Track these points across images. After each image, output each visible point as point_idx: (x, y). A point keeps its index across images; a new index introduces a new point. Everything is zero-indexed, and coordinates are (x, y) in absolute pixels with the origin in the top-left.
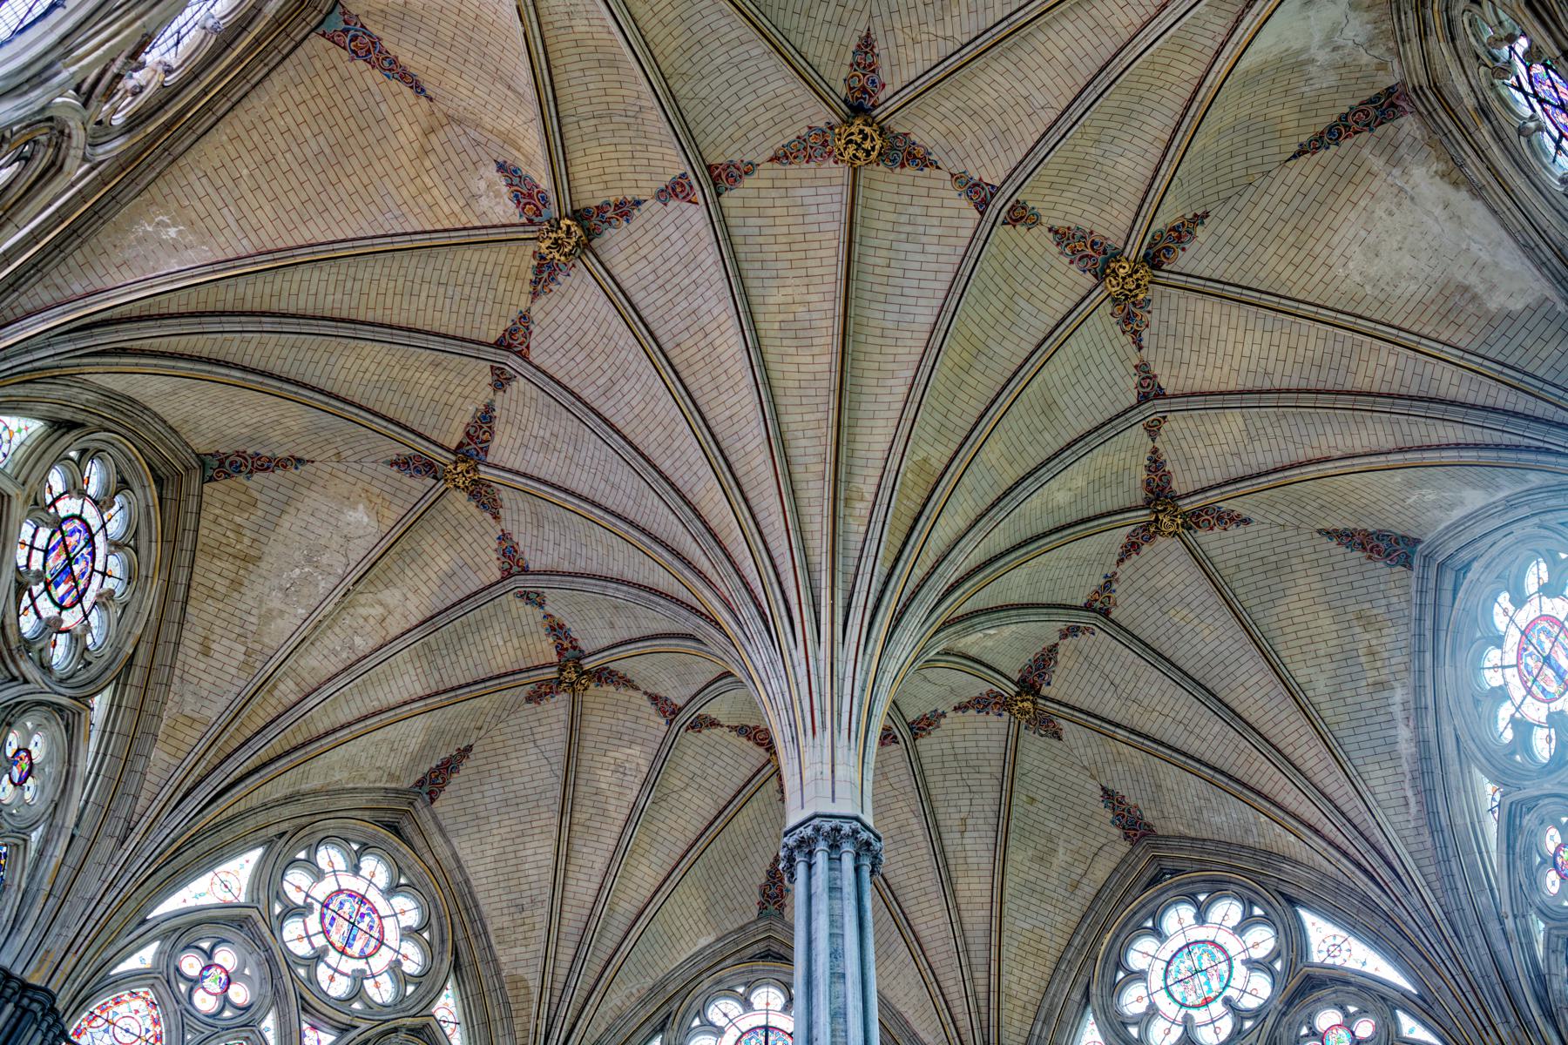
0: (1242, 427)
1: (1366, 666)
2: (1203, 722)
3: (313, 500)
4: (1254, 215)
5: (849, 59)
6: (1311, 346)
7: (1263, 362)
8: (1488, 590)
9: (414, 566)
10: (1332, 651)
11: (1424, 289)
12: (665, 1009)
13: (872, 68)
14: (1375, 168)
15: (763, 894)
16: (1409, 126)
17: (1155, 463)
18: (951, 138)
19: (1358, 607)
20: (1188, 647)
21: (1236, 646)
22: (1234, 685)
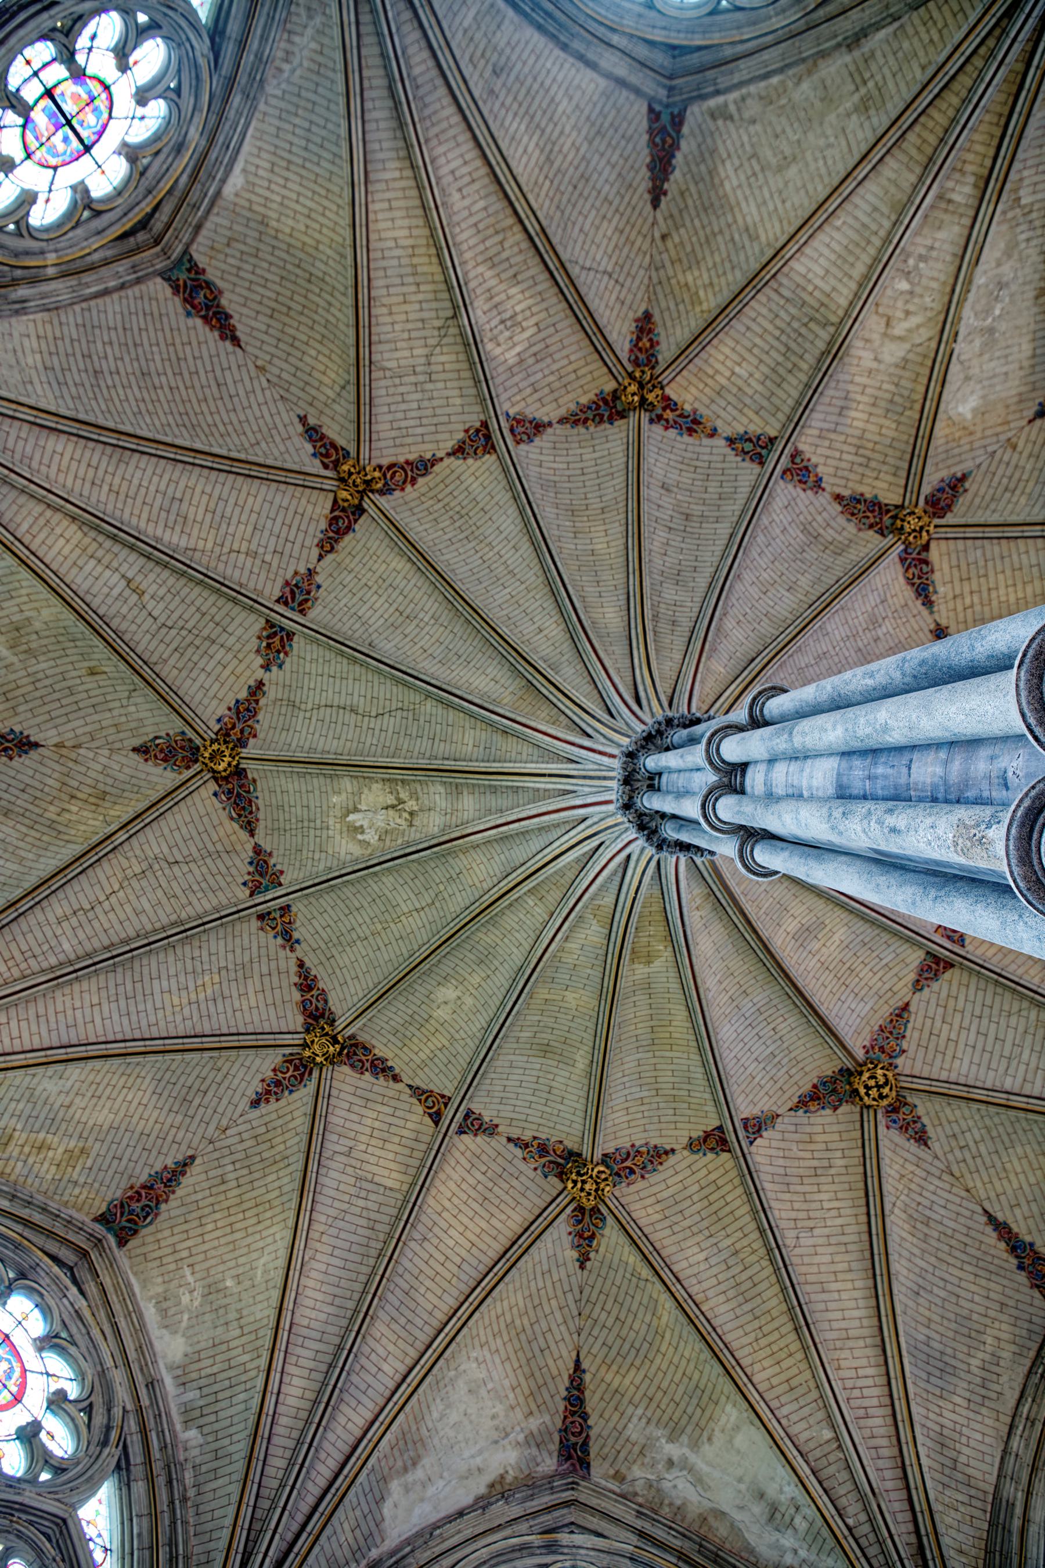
0: (377, 1179)
1: (33, 1136)
2: (82, 936)
3: (1011, 388)
4: (554, 1302)
5: (925, 1120)
6: (429, 1295)
7: (435, 1241)
8: (52, 1303)
9: (888, 396)
10: (71, 1111)
11: (430, 1425)
13: (904, 1128)
14: (531, 1420)
15: (208, 285)
16: (549, 1464)
17: (381, 1068)
18: (807, 1138)
19: (93, 1154)
20: (172, 972)
21: (144, 1023)
22: (104, 994)
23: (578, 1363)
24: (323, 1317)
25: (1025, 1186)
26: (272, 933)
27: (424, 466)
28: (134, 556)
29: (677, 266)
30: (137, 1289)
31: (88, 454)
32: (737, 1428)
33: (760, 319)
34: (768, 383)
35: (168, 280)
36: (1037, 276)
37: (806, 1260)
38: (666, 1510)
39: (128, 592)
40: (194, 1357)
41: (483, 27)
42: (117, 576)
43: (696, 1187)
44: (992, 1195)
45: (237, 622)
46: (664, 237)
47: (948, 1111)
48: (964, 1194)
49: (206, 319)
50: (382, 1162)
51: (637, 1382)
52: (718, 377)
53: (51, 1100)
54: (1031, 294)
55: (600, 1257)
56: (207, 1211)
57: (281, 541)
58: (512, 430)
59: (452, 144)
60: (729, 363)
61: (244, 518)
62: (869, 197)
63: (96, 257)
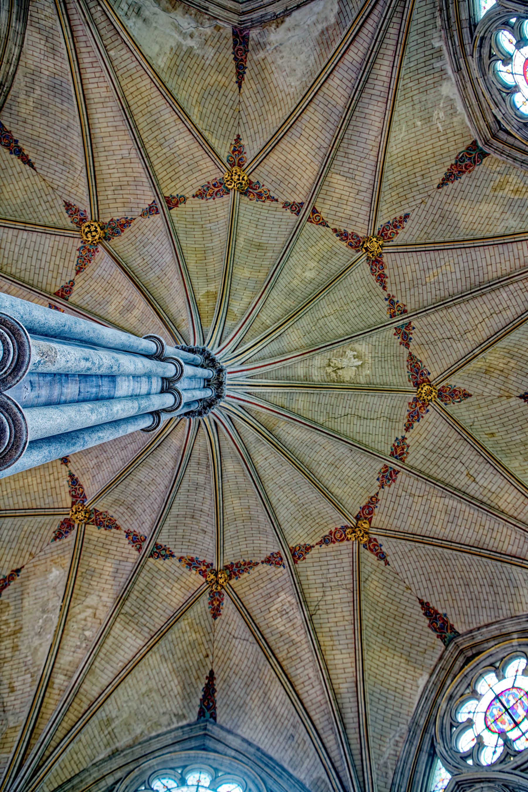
0: (344, 179)
1: (521, 197)
3: (32, 584)
5: (66, 215)
6: (317, 119)
7: (314, 147)
8: (510, 111)
9: (94, 579)
10: (501, 210)
12: (428, 737)
13: (77, 210)
14: (263, 57)
15: (435, 630)
16: (254, 34)
17: (343, 236)
18: (126, 205)
19: (490, 189)
20: (450, 282)
21: (464, 256)
22: (485, 271)
23: (240, 87)
24: (371, 107)
25: (15, 182)
26: (399, 303)
27: (325, 541)
28: (472, 493)
29: (200, 642)
30: (466, 119)
31: (496, 545)
32: (158, 55)
33: (159, 616)
34: (154, 584)
35: (456, 632)
36: (22, 639)
37: (125, 142)
38: (193, 12)
39: (475, 475)
40: (437, 84)
41: (299, 759)
42: (480, 483)
43: (181, 178)
44: (31, 178)
45: (419, 462)
46: (207, 656)
47: (55, 220)
48: (46, 178)
49: (436, 612)
50: (342, 187)
51: (209, 77)
52: (179, 587)
53: (512, 216)
54: (24, 630)
55: (230, 141)
56: (432, 160)
57: (397, 502)
58: (282, 559)
59: (314, 701)
60: (174, 594)
61: (416, 513)
62: (106, 677)
63: (492, 643)
